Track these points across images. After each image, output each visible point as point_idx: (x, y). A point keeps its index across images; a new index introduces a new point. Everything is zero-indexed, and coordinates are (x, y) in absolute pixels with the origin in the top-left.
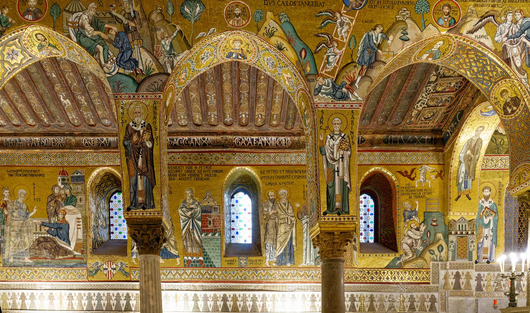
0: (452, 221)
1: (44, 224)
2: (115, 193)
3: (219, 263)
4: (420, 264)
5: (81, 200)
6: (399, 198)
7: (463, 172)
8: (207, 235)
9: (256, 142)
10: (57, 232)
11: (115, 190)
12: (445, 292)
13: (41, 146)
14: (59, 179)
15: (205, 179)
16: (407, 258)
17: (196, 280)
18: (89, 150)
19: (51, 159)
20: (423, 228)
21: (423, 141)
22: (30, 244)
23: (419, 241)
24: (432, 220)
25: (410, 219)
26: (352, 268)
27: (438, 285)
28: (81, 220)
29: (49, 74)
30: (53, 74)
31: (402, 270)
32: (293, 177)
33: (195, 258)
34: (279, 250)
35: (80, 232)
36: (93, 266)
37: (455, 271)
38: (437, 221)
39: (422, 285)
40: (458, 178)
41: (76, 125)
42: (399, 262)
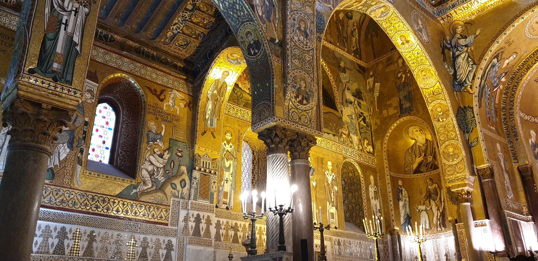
0: (197, 156)
4: (160, 198)
6: (144, 115)
7: (210, 109)
12: (184, 238)
16: (145, 188)
20: (167, 156)
21: (175, 67)
23: (162, 170)
24: (177, 149)
25: (154, 142)
26: (71, 188)
27: (176, 228)
31: (138, 203)
32: (7, 44)
37: (196, 213)
38: (182, 151)
39: (159, 226)
40: (205, 113)
42: (134, 191)
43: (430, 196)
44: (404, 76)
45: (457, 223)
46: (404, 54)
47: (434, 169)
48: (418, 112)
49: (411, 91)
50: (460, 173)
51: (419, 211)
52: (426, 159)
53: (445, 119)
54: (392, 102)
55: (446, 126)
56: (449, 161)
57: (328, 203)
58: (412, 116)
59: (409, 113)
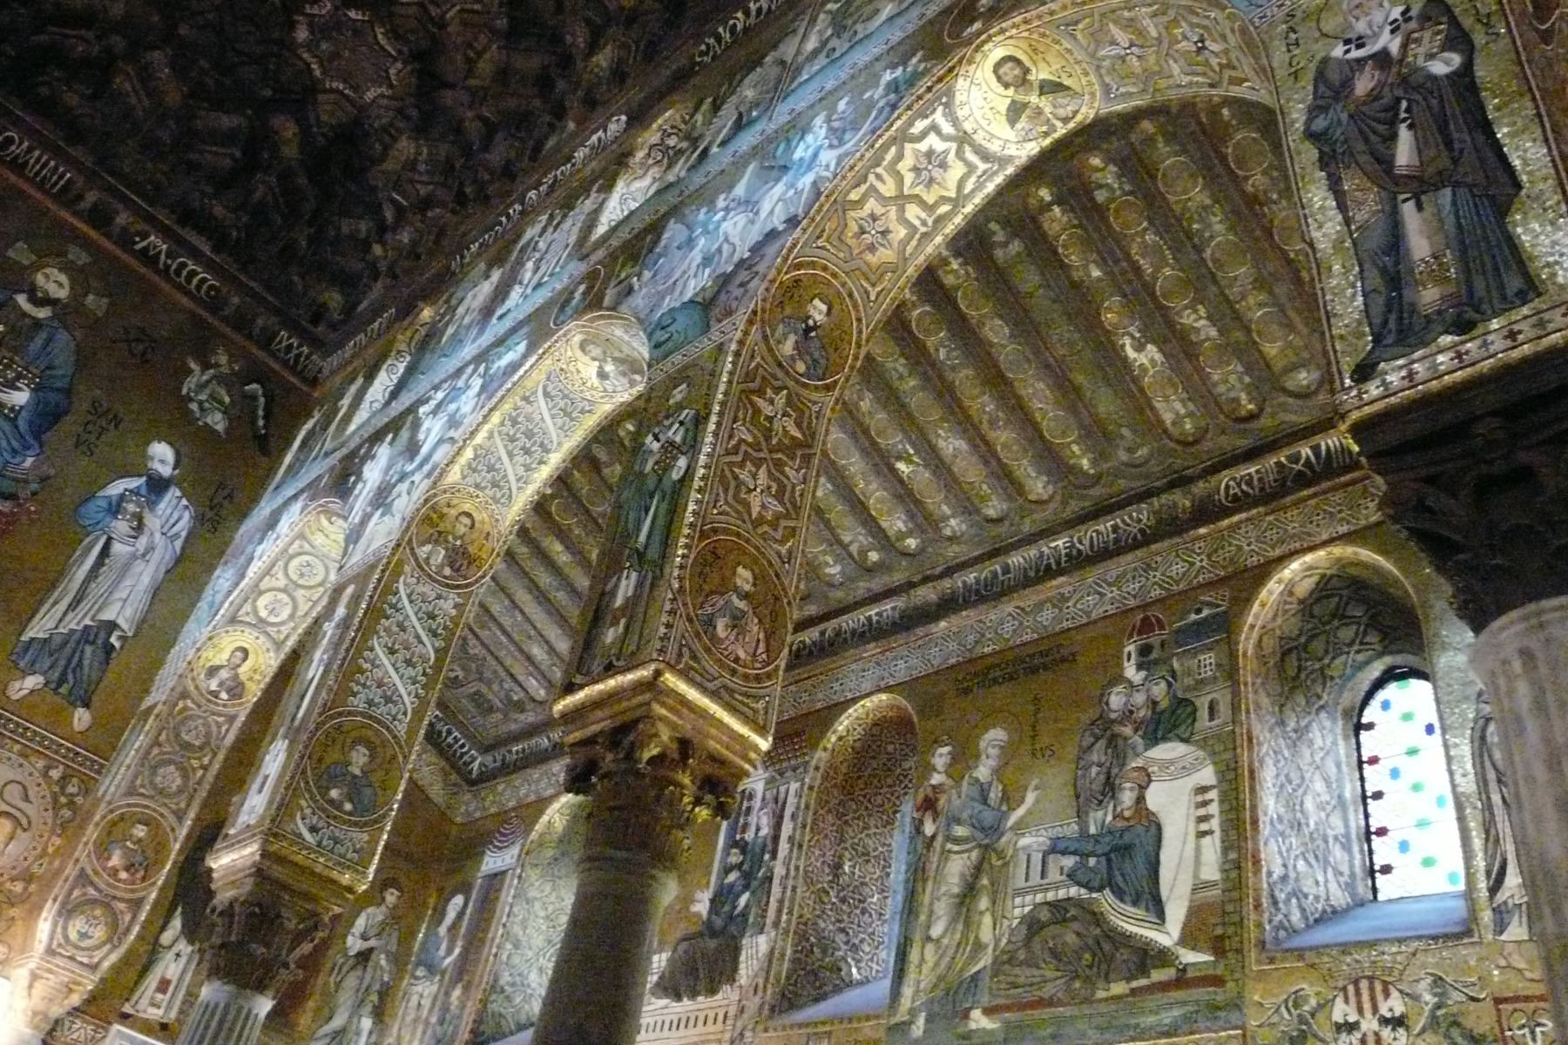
1: (1062, 845)
2: (1379, 684)
5: (1212, 710)
10: (1110, 868)
11: (1376, 670)
13: (1077, 562)
14: (1129, 654)
18: (1243, 516)
19: (1102, 595)
22: (996, 945)
28: (1213, 795)
29: (1076, 275)
30: (1092, 266)
35: (1211, 849)
36: (1275, 1019)
41: (1191, 439)
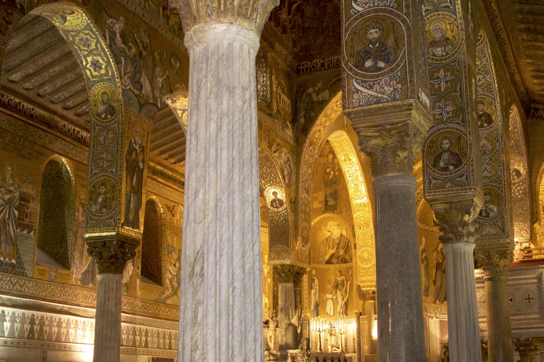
3: (31, 271)
8: (22, 230)
9: (76, 133)
15: (27, 158)
17: (6, 291)
33: (7, 260)
34: (84, 266)
43: (336, 287)
44: (332, 173)
45: (361, 315)
46: (344, 168)
47: (344, 263)
48: (341, 213)
49: (337, 190)
50: (371, 276)
51: (326, 299)
52: (338, 252)
53: (365, 228)
54: (319, 196)
55: (366, 234)
56: (363, 264)
57: (264, 294)
58: (336, 214)
59: (333, 211)
